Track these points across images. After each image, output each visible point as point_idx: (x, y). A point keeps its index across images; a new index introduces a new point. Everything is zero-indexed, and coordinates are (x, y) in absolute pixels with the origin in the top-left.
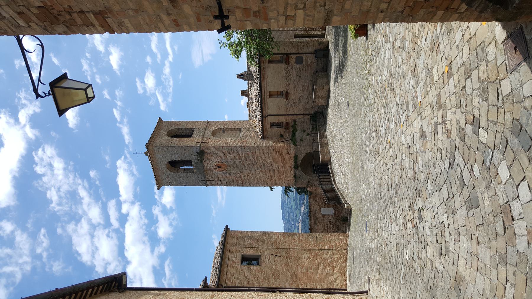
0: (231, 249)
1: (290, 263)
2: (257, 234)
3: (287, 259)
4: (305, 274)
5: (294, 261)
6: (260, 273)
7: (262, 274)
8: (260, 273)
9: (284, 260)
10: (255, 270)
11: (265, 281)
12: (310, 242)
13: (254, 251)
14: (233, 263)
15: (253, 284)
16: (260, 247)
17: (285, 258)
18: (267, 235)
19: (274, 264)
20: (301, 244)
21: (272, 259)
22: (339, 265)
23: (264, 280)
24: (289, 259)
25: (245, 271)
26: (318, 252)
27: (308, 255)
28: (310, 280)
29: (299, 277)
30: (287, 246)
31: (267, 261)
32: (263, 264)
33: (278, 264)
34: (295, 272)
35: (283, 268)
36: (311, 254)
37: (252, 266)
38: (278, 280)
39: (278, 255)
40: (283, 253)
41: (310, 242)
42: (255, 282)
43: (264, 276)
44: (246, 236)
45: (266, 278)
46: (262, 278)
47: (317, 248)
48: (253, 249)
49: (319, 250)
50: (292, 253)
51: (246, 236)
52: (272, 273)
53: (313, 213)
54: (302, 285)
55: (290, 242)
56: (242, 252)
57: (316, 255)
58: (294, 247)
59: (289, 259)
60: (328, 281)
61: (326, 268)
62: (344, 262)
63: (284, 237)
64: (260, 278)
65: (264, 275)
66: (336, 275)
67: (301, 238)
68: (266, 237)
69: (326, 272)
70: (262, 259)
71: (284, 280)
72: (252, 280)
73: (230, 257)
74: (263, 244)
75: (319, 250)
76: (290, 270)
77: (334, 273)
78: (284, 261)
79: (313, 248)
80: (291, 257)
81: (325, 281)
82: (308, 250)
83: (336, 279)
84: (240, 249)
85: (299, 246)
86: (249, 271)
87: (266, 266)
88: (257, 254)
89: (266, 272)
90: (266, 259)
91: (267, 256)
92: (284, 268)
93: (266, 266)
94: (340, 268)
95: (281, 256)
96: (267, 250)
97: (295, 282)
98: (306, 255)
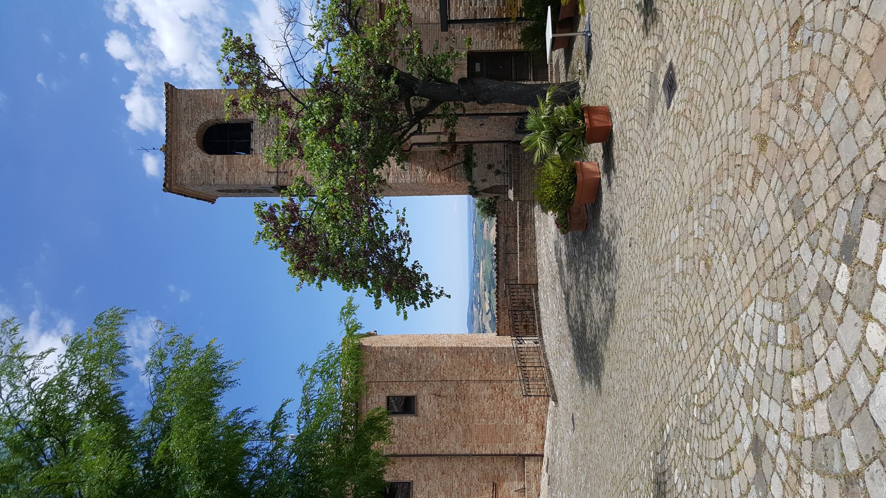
1: (461, 407)
3: (458, 401)
5: (468, 404)
6: (417, 428)
7: (420, 431)
8: (417, 428)
9: (453, 403)
11: (425, 443)
12: (494, 366)
13: (405, 387)
15: (408, 448)
16: (415, 379)
17: (455, 399)
18: (424, 354)
19: (437, 410)
20: (480, 371)
22: (536, 409)
23: (424, 442)
26: (505, 386)
27: (490, 391)
28: (492, 438)
29: (474, 434)
30: (458, 375)
31: (426, 405)
32: (421, 412)
34: (470, 425)
35: (451, 417)
36: (495, 389)
37: (404, 417)
38: (444, 439)
39: (443, 393)
40: (451, 390)
41: (494, 366)
42: (410, 445)
44: (390, 359)
47: (504, 378)
48: (404, 383)
49: (507, 381)
51: (390, 359)
54: (479, 447)
55: (462, 368)
56: (387, 392)
57: (503, 391)
58: (469, 377)
61: (516, 416)
62: (544, 404)
63: (452, 357)
64: (418, 437)
65: (423, 432)
66: (530, 427)
67: (480, 358)
68: (423, 358)
69: (515, 423)
70: (419, 402)
71: (453, 440)
72: (406, 442)
73: (368, 402)
74: (419, 374)
75: (507, 381)
76: (462, 420)
77: (528, 425)
79: (498, 377)
80: (463, 397)
81: (513, 439)
82: (491, 381)
83: (529, 436)
86: (400, 427)
87: (425, 417)
88: (409, 394)
90: (426, 404)
91: (426, 397)
93: (425, 417)
94: (537, 414)
96: (425, 385)
97: (469, 442)
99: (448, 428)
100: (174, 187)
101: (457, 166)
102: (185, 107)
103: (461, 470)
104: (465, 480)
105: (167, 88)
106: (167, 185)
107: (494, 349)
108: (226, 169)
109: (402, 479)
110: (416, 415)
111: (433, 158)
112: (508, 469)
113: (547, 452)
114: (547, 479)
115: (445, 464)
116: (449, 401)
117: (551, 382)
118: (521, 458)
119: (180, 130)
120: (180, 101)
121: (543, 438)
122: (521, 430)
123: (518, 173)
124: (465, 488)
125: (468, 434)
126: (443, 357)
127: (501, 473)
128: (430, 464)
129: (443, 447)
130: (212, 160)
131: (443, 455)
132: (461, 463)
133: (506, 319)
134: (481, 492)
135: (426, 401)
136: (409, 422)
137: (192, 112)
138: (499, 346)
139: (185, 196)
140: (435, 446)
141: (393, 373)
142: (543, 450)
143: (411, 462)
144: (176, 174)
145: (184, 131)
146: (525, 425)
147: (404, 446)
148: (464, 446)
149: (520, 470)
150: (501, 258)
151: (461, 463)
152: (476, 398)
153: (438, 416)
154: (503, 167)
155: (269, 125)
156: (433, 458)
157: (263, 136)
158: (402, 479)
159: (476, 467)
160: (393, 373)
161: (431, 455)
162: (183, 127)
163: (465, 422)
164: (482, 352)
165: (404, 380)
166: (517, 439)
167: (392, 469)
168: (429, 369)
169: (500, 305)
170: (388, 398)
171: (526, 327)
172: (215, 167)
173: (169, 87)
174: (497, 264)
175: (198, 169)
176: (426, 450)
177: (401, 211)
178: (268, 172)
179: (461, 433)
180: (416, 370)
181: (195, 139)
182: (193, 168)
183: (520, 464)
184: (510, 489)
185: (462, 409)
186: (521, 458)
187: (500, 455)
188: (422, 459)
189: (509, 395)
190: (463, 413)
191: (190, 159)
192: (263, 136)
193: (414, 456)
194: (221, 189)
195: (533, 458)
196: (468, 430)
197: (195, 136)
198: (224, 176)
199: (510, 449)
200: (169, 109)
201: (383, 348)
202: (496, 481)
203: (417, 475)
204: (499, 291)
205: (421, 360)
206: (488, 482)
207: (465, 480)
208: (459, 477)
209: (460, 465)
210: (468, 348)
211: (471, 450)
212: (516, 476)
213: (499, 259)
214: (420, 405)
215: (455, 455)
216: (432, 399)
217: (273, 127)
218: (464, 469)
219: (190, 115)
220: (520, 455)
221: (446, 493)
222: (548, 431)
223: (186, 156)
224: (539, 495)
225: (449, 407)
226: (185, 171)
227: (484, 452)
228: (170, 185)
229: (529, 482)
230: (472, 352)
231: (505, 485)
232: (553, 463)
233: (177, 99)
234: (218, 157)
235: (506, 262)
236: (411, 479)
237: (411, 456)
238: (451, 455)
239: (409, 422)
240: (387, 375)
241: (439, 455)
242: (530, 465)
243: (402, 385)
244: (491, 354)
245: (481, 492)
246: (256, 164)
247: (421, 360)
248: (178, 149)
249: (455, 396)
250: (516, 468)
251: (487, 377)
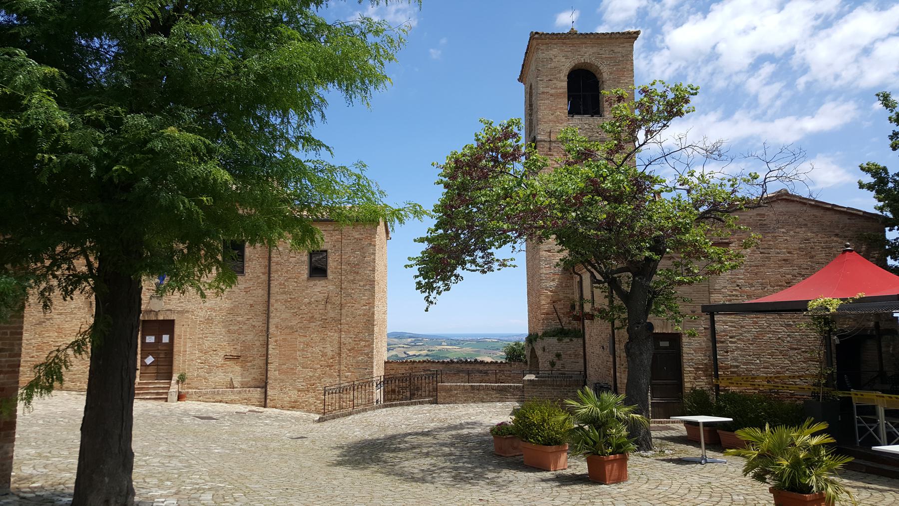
0: (337, 232)
2: (370, 270)
3: (321, 321)
4: (295, 347)
5: (318, 331)
6: (296, 280)
7: (293, 283)
9: (319, 316)
10: (299, 273)
12: (354, 357)
13: (336, 268)
15: (277, 271)
16: (343, 277)
17: (323, 317)
18: (367, 287)
19: (312, 300)
20: (350, 343)
22: (311, 400)
23: (283, 287)
25: (298, 257)
26: (335, 369)
27: (330, 354)
29: (289, 337)
30: (347, 321)
31: (318, 289)
32: (312, 283)
33: (313, 307)
34: (297, 333)
37: (307, 267)
38: (284, 307)
39: (329, 306)
40: (332, 314)
41: (354, 357)
42: (279, 273)
43: (291, 287)
44: (364, 253)
45: (286, 290)
46: (286, 284)
47: (343, 368)
48: (339, 267)
49: (339, 371)
51: (364, 253)
52: (295, 298)
54: (276, 341)
55: (353, 325)
56: (332, 250)
57: (330, 366)
58: (345, 332)
60: (282, 381)
61: (305, 379)
62: (316, 409)
63: (364, 315)
65: (291, 285)
66: (294, 394)
67: (363, 343)
69: (298, 378)
70: (321, 282)
71: (283, 316)
72: (282, 269)
75: (339, 371)
77: (296, 392)
78: (317, 316)
79: (344, 362)
80: (324, 326)
81: (282, 377)
84: (338, 246)
85: (346, 339)
86: (298, 263)
87: (307, 288)
88: (329, 272)
89: (296, 288)
90: (320, 287)
91: (325, 288)
92: (305, 316)
94: (306, 401)
95: (326, 311)
97: (280, 332)
99: (294, 311)
100: (535, 42)
101: (558, 321)
102: (616, 51)
103: (253, 324)
104: (245, 327)
105: (635, 33)
106: (537, 36)
107: (372, 358)
108: (553, 91)
109: (247, 265)
110: (308, 279)
111: (566, 297)
112: (253, 371)
113: (268, 411)
114: (242, 411)
115: (260, 308)
116: (321, 311)
117: (338, 417)
118: (264, 385)
119: (592, 47)
120: (621, 45)
121: (282, 408)
122: (291, 385)
123: (553, 385)
124: (236, 328)
125: (288, 331)
126: (364, 306)
127: (249, 364)
128: (261, 292)
129: (275, 305)
130: (562, 78)
131: (268, 306)
132: (260, 324)
133: (402, 370)
134: (232, 343)
135: (322, 289)
136: (302, 272)
137: (610, 58)
138: (375, 364)
139: (526, 53)
140: (278, 298)
141: (350, 256)
142: (270, 407)
143: (264, 274)
144: (548, 44)
145: (591, 51)
146: (295, 388)
147: (279, 267)
148: (277, 327)
149: (252, 383)
150: (464, 367)
151: (260, 324)
152: (323, 339)
153: (306, 300)
154: (559, 370)
155: (598, 133)
156: (266, 296)
157: (586, 126)
158: (247, 265)
159: (256, 338)
160: (350, 256)
161: (269, 294)
162: (595, 50)
163: (301, 328)
164: (369, 346)
165: (343, 267)
166: (282, 381)
167: (257, 256)
168: (353, 291)
169: (415, 365)
170: (326, 251)
171: (393, 391)
172: (555, 81)
173: (635, 35)
174: (457, 362)
175: (553, 65)
176: (274, 290)
177: (513, 263)
178: (550, 132)
179: (290, 324)
180: (352, 278)
181: (583, 61)
182: (554, 60)
183: (257, 384)
184: (235, 373)
185: (313, 324)
186: (264, 384)
187: (267, 363)
188: (265, 285)
189: (325, 373)
190: (309, 326)
191: (563, 57)
192: (586, 126)
193: (269, 277)
194: (533, 87)
195: (264, 397)
196: (292, 330)
197: (586, 61)
198: (545, 90)
199: (273, 374)
200: (613, 36)
201: (375, 246)
202: (241, 359)
203: (251, 280)
204: (429, 364)
205: (362, 283)
206: (242, 351)
207: (245, 327)
208: (247, 322)
209: (259, 323)
210: (373, 331)
211: (273, 334)
212: (246, 380)
213: (463, 364)
214: (318, 283)
215: (268, 317)
217: (597, 136)
218: (254, 326)
219: (607, 56)
220: (266, 383)
221: (232, 309)
222: (289, 412)
223: (566, 53)
224: (227, 403)
225: (315, 311)
226: (551, 52)
227: (270, 346)
228: (537, 39)
229: (240, 392)
230: (369, 335)
231: (238, 369)
232: (258, 417)
233: (623, 43)
234: (565, 84)
235: (459, 371)
236: (247, 274)
237: (269, 274)
238: (268, 314)
239: (302, 272)
240: (348, 249)
241: (269, 301)
242: (257, 393)
243: (338, 265)
244: (367, 354)
245: (232, 343)
246: (558, 121)
247: (362, 283)
248: (573, 45)
250: (254, 379)
251: (344, 350)
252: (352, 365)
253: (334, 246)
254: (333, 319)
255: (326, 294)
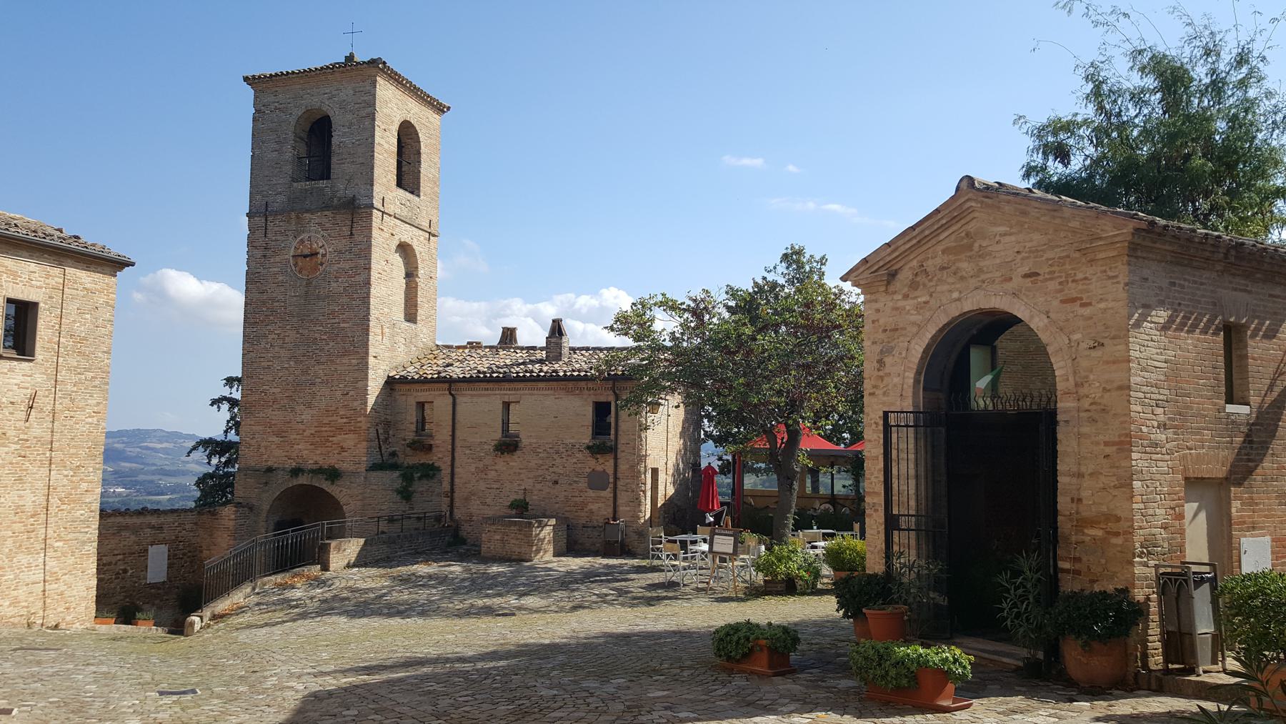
1: (6, 449)
5: (11, 463)
9: (14, 433)
14: (14, 274)
16: (61, 360)
17: (22, 436)
21: (22, 396)
24: (18, 447)
27: (29, 508)
31: (18, 379)
47: (50, 531)
50: (38, 458)
53: (153, 520)
55: (72, 451)
56: (46, 304)
59: (18, 447)
78: (11, 433)
80: (23, 453)
95: (27, 424)
96: (48, 379)
98: (31, 499)
126: (89, 417)
141: (74, 321)
160: (74, 321)
168: (75, 389)
205: (90, 375)
216: (25, 391)
247: (90, 375)
249: (26, 437)
251: (54, 501)
252: (65, 528)
253: (51, 297)
254: (38, 439)
255: (29, 391)
